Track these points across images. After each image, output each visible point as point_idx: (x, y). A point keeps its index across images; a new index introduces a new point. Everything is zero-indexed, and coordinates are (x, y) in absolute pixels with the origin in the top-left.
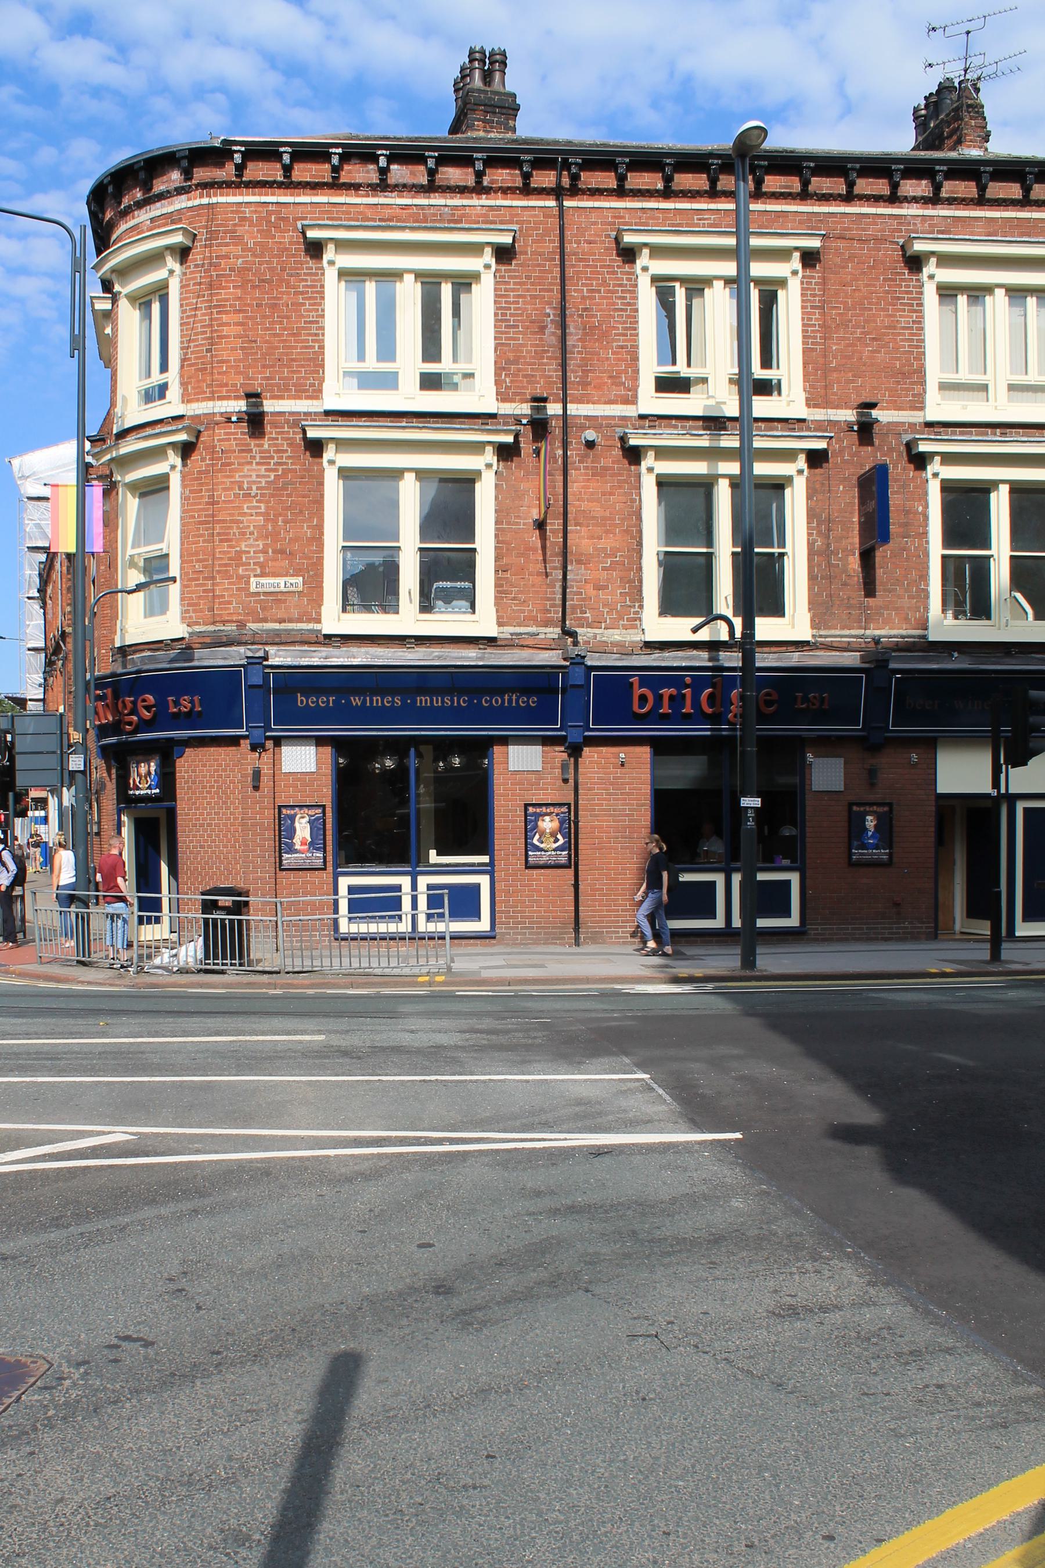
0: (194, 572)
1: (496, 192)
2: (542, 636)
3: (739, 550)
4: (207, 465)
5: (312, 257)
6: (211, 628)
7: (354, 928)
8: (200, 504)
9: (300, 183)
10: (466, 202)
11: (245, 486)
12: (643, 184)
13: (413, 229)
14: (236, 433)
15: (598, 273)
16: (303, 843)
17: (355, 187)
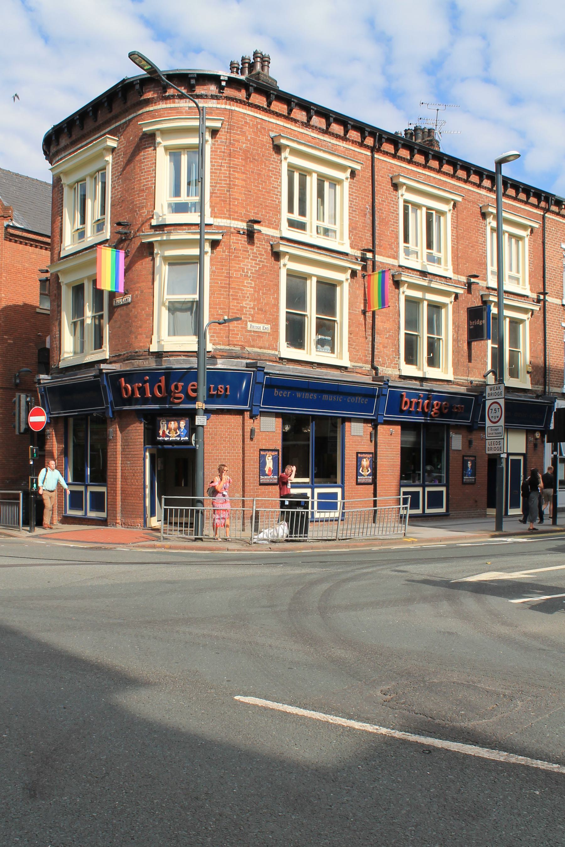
0: (218, 315)
1: (349, 142)
2: (364, 368)
3: (496, 346)
4: (226, 255)
5: (275, 153)
6: (227, 347)
7: (322, 515)
8: (222, 276)
9: (273, 112)
10: (338, 143)
11: (245, 271)
12: (403, 155)
13: (324, 151)
14: (241, 240)
15: (385, 193)
16: (269, 470)
17: (295, 121)
